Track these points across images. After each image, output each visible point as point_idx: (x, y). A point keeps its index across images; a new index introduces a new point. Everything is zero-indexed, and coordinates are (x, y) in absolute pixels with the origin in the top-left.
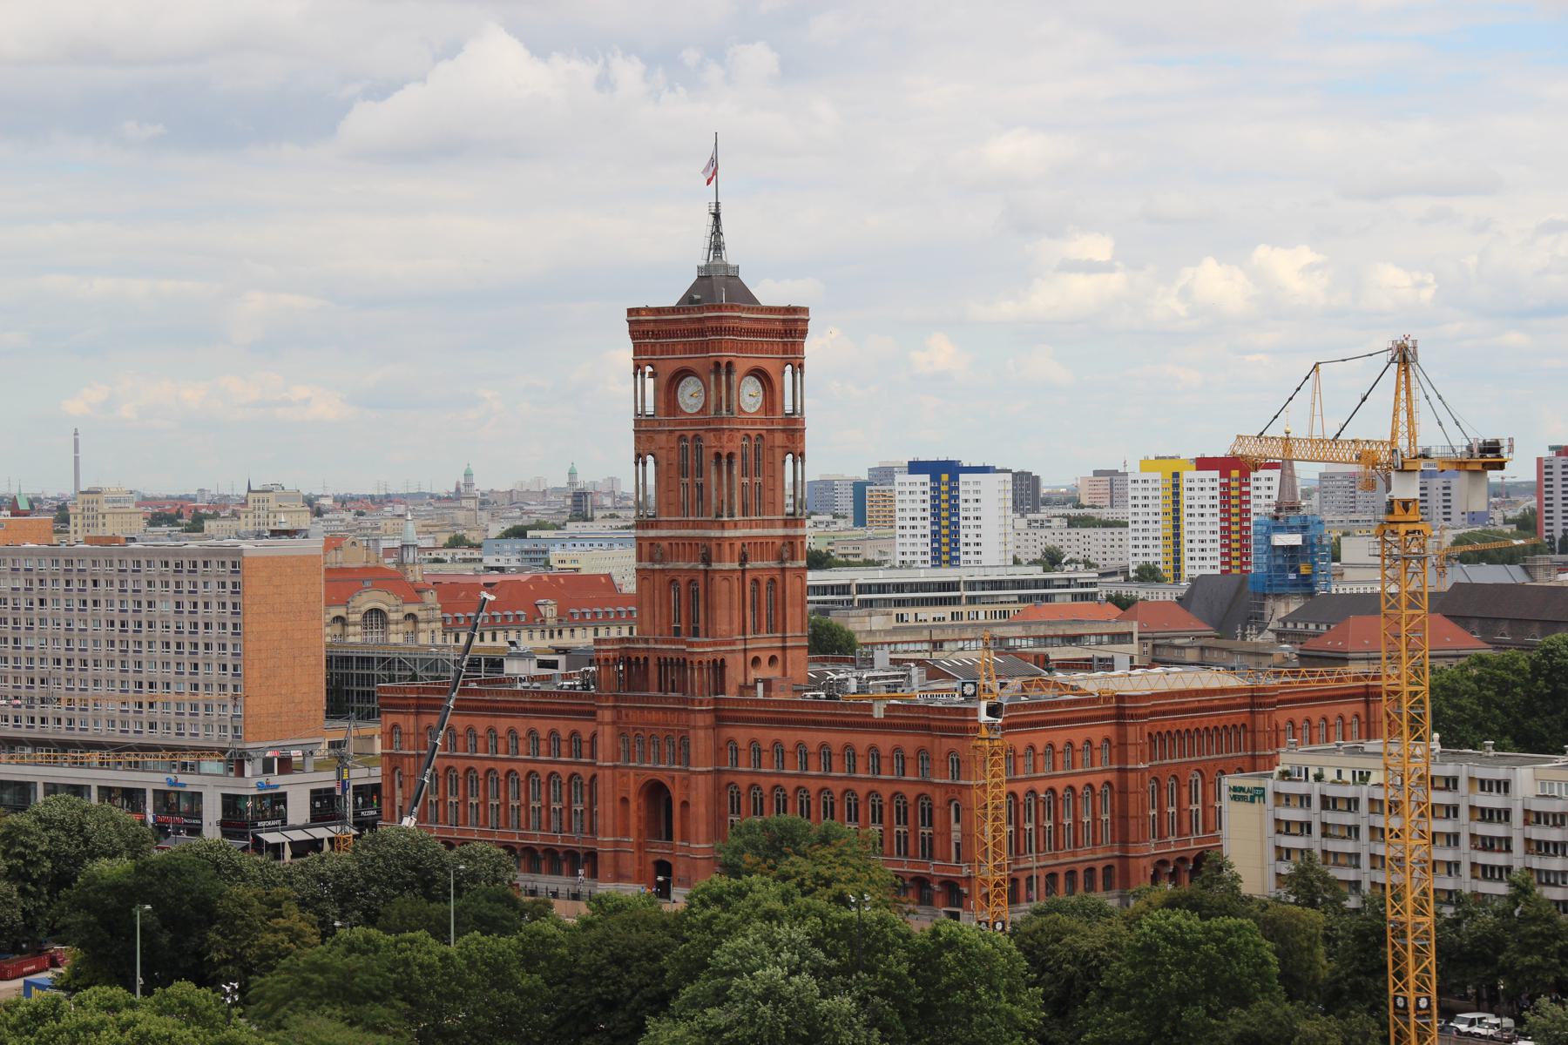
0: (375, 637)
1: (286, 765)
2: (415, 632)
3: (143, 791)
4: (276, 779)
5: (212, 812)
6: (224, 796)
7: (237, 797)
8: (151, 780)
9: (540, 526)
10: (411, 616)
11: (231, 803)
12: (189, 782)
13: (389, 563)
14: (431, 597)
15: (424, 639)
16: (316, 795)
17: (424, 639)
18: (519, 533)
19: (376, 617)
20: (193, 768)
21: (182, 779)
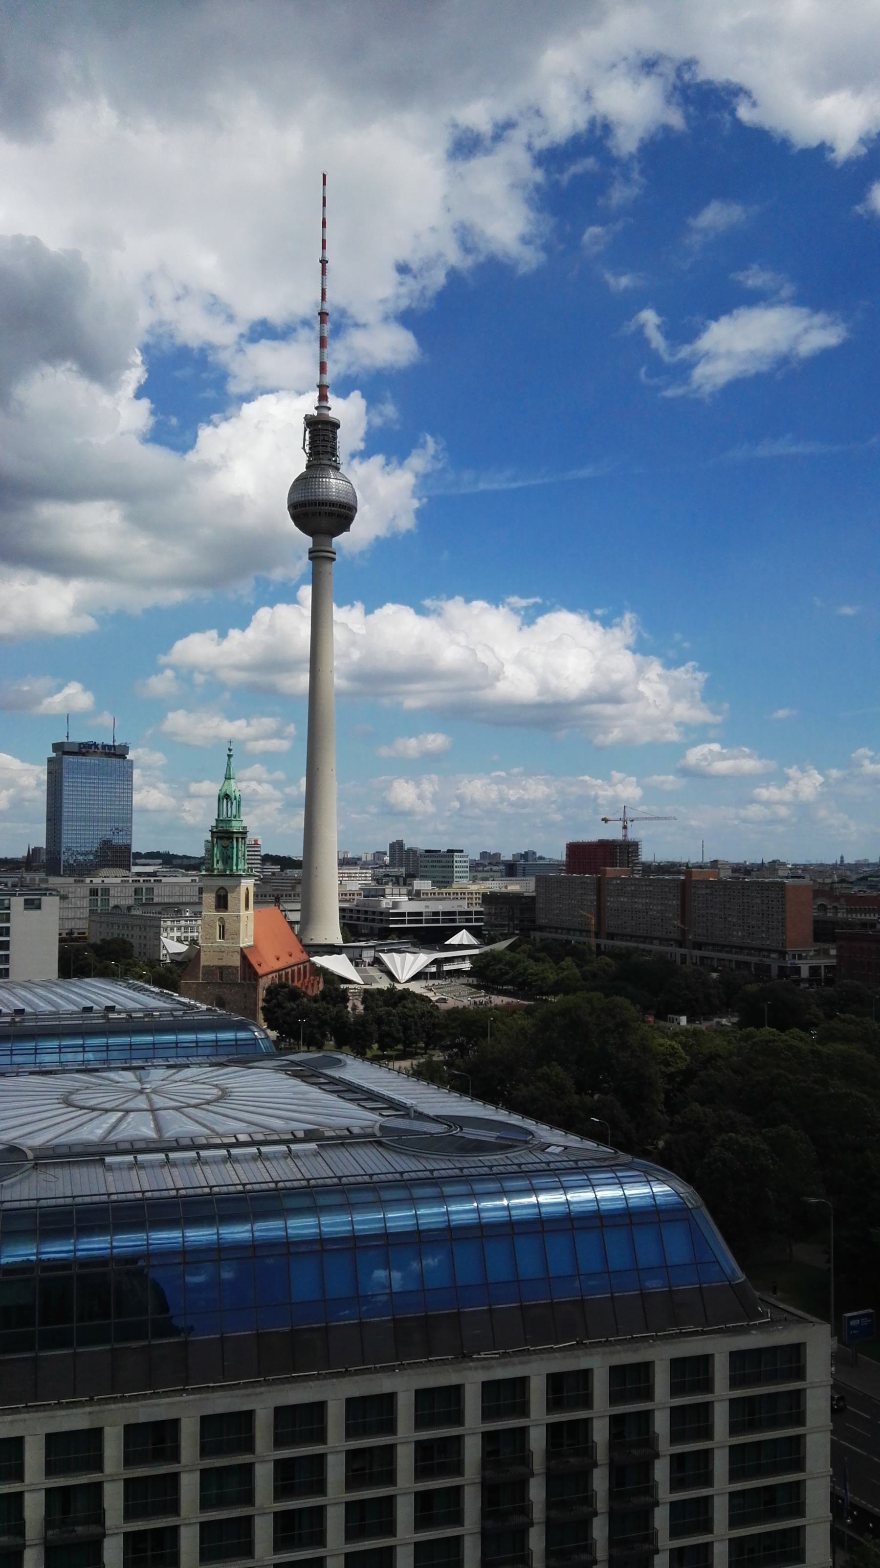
0: (821, 914)
1: (800, 957)
2: (837, 913)
3: (750, 963)
4: (797, 962)
5: (775, 971)
6: (779, 967)
7: (783, 967)
8: (754, 959)
9: (871, 876)
10: (835, 907)
11: (781, 969)
12: (767, 961)
13: (827, 888)
14: (843, 901)
15: (840, 915)
16: (811, 968)
17: (840, 915)
18: (865, 878)
19: (822, 907)
20: (768, 957)
21: (764, 959)
